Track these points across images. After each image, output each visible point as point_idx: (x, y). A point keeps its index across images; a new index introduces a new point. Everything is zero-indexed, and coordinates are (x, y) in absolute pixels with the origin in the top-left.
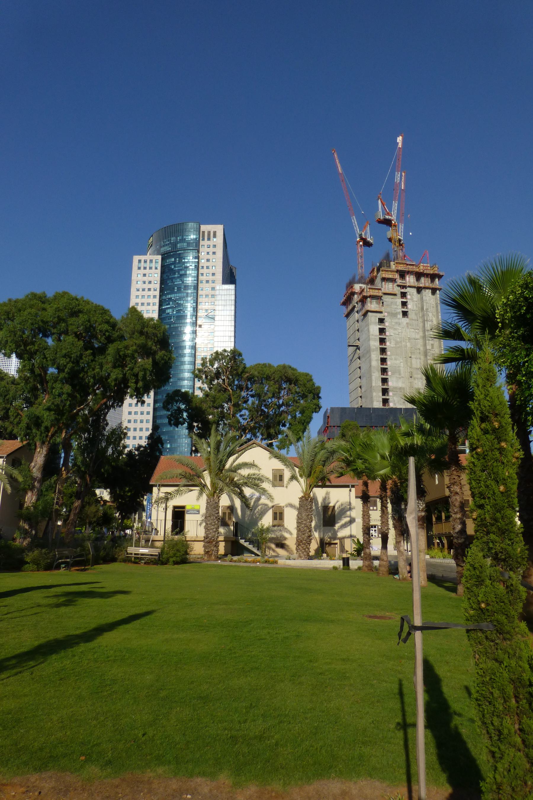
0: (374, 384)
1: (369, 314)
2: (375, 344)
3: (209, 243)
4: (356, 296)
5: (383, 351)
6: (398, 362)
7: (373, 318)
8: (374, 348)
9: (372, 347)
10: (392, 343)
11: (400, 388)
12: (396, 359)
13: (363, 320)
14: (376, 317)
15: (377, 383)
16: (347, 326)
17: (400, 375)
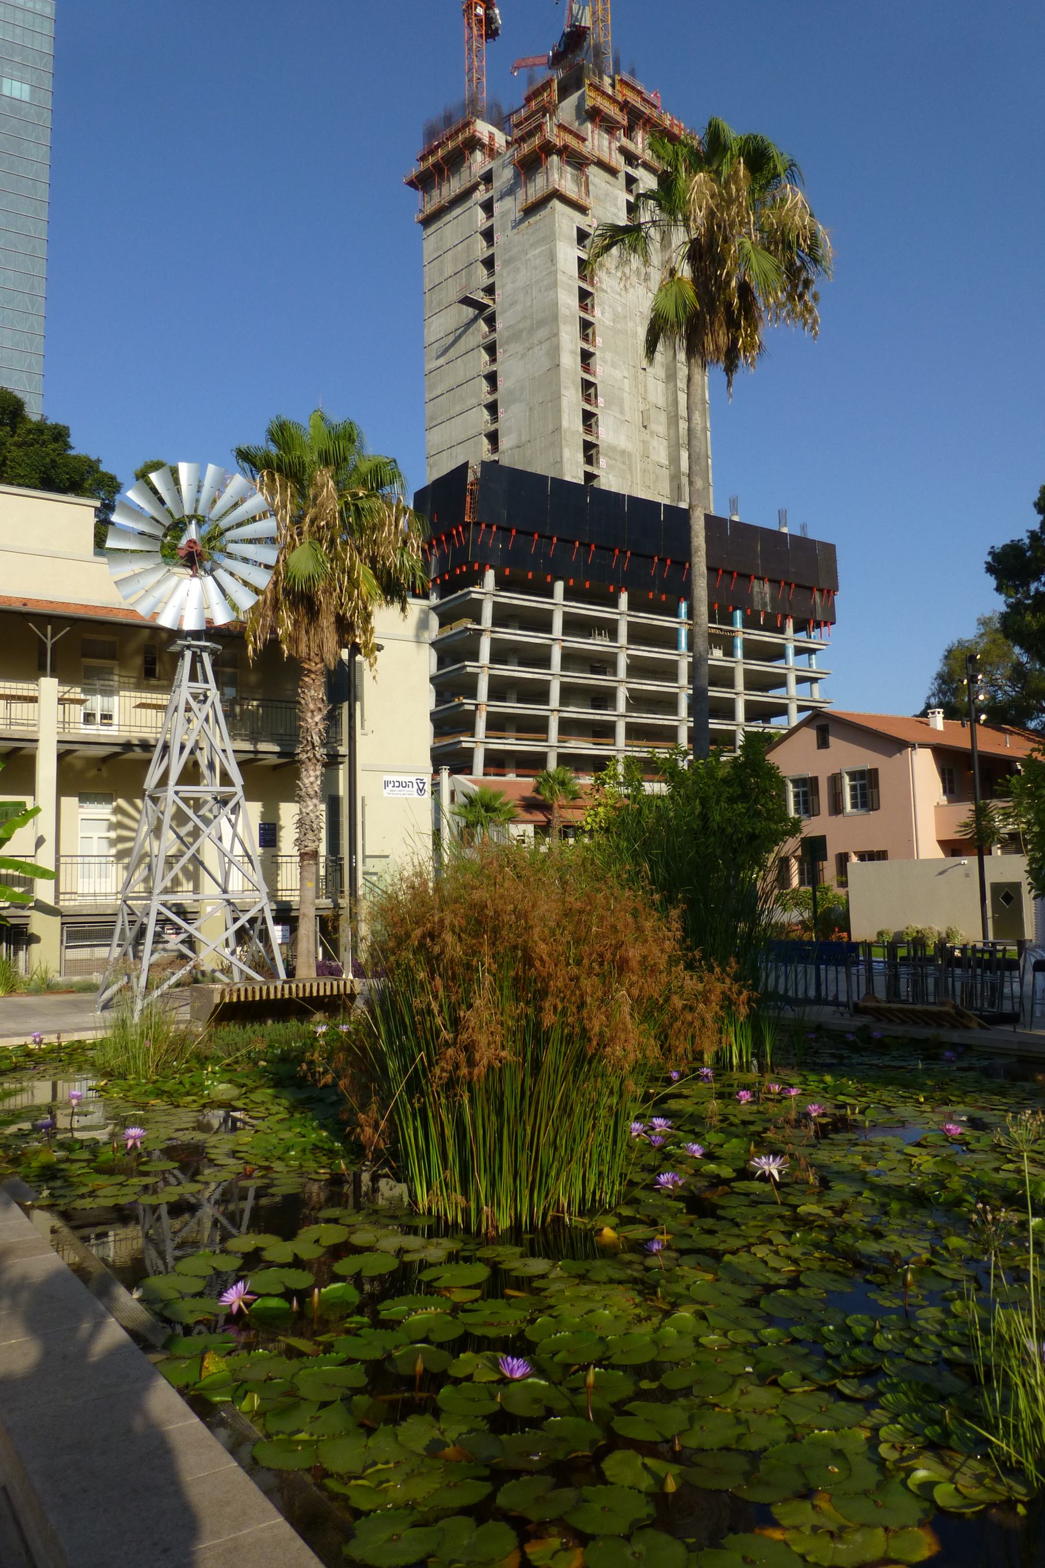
0: (565, 424)
1: (556, 203)
2: (568, 301)
4: (478, 155)
5: (586, 325)
6: (618, 374)
7: (564, 220)
8: (567, 312)
9: (563, 311)
10: (607, 315)
11: (623, 452)
12: (614, 365)
14: (572, 219)
15: (572, 422)
17: (622, 412)
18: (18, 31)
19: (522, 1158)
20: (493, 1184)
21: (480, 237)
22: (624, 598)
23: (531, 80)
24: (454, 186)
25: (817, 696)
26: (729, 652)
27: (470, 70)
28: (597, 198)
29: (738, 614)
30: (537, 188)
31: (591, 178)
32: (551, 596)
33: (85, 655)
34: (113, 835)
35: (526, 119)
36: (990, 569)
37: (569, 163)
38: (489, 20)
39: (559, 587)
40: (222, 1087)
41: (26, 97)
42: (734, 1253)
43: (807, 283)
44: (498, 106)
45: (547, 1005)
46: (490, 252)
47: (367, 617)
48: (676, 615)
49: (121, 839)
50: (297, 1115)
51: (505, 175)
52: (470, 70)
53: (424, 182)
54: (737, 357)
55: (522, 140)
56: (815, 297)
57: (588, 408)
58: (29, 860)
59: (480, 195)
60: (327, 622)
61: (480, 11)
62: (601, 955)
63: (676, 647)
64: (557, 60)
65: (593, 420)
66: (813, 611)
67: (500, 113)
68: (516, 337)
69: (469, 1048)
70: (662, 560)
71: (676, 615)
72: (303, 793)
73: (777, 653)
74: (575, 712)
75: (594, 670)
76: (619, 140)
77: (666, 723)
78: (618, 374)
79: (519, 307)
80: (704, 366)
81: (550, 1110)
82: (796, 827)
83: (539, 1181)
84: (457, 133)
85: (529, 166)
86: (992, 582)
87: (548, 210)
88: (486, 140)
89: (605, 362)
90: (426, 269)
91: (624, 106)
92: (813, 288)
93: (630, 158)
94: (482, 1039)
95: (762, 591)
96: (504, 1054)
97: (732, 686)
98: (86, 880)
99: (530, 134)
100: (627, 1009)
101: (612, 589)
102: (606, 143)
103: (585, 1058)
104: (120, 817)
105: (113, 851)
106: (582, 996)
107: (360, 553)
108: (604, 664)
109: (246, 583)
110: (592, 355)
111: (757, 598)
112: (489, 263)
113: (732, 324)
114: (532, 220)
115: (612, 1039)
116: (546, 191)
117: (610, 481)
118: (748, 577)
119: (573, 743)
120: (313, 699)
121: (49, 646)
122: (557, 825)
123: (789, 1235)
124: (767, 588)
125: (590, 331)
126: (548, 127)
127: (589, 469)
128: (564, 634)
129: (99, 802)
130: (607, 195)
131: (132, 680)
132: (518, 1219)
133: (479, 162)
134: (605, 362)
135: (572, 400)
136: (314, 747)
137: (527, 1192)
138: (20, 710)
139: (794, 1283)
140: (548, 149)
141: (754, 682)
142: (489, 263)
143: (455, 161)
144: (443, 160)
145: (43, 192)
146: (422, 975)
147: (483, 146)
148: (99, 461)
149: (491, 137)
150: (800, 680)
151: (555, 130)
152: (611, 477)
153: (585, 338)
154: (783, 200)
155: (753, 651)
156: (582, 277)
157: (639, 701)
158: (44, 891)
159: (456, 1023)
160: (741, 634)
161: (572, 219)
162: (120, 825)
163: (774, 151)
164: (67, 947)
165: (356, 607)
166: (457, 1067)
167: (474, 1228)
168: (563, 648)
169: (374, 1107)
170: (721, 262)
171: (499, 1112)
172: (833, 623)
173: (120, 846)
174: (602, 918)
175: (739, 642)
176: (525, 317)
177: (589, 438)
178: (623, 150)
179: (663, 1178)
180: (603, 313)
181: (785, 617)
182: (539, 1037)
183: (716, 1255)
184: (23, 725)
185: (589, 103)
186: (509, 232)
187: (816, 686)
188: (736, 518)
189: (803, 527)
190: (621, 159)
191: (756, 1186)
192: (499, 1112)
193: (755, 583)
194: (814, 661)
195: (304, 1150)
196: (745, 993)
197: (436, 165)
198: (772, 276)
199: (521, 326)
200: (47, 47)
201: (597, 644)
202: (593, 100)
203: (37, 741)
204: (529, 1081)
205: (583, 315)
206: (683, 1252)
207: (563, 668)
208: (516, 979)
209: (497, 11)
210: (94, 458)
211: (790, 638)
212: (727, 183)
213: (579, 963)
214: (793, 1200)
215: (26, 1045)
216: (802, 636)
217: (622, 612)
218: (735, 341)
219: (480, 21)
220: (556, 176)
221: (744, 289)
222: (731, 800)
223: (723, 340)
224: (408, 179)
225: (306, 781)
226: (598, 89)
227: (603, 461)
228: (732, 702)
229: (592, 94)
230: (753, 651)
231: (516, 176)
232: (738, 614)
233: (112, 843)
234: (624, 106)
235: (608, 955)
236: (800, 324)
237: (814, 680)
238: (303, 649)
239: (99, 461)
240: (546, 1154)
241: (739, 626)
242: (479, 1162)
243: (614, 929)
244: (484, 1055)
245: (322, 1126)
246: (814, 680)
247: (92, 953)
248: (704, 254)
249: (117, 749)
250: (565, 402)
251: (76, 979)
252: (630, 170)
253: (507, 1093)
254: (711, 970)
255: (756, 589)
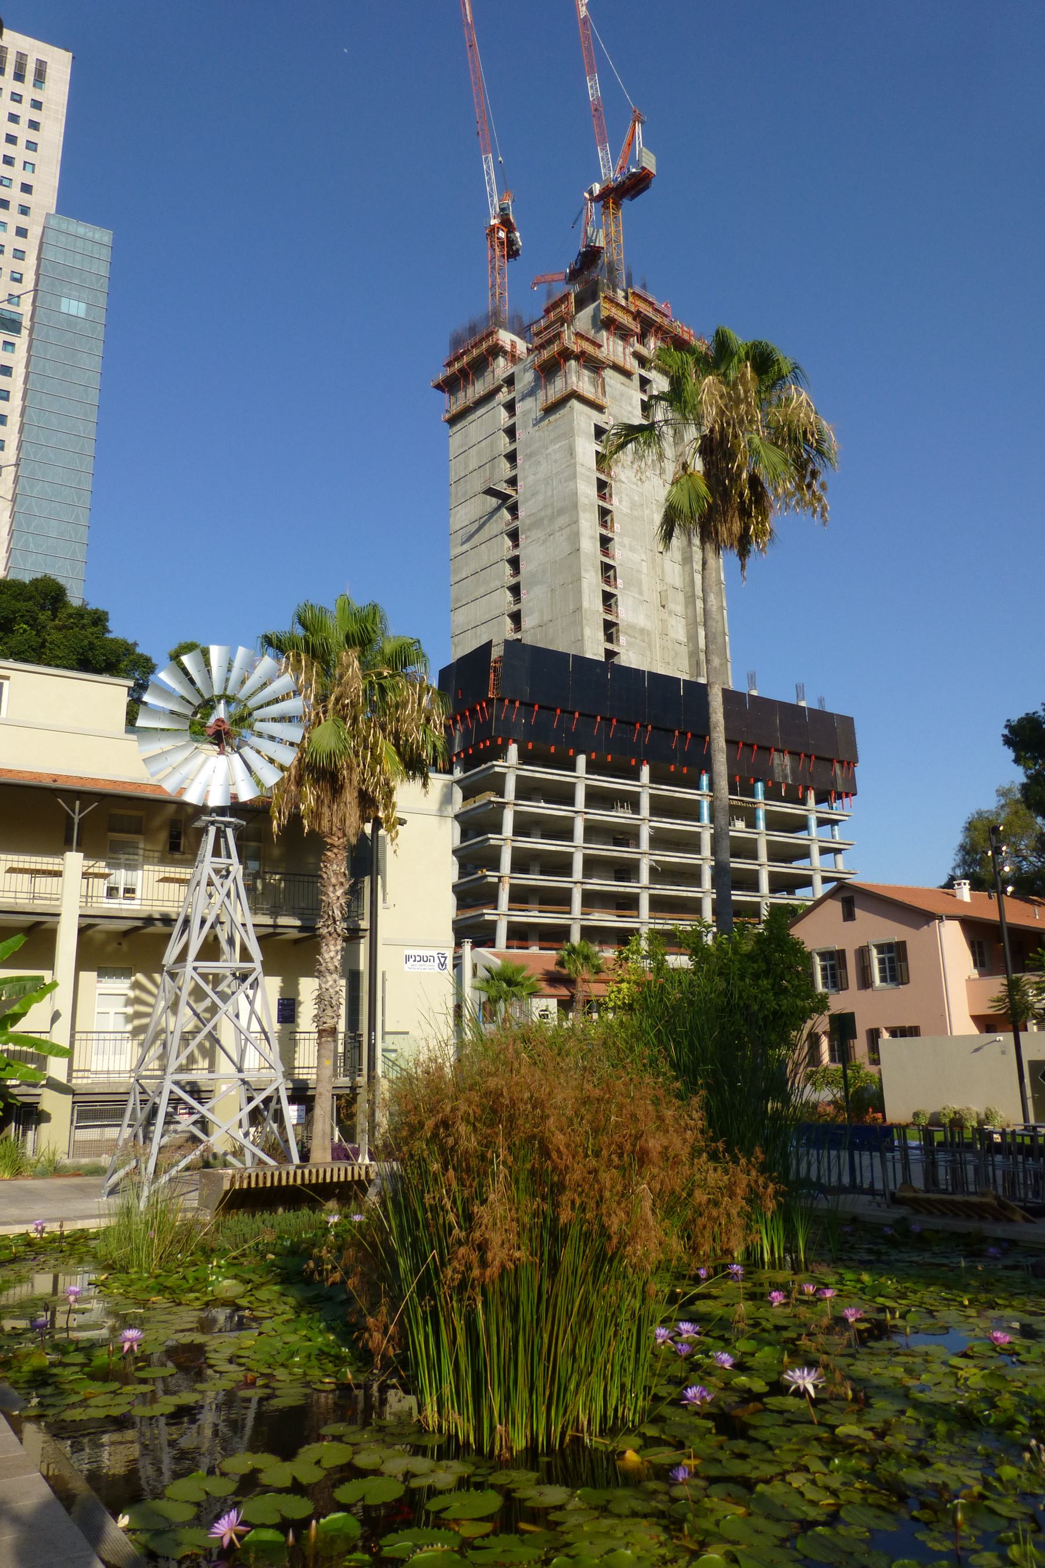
0: (586, 604)
1: (575, 403)
2: (587, 491)
3: (18, 87)
4: (501, 361)
5: (604, 513)
6: (636, 558)
7: (583, 418)
8: (586, 501)
9: (582, 500)
11: (642, 631)
12: (632, 549)
13: (538, 422)
14: (589, 417)
16: (452, 449)
17: (641, 593)
18: (78, 257)
19: (539, 1371)
20: (507, 1399)
21: (503, 434)
22: (645, 771)
23: (549, 295)
24: (478, 388)
25: (841, 867)
26: (752, 824)
27: (493, 286)
28: (613, 398)
29: (760, 786)
30: (557, 389)
31: (607, 380)
32: (574, 770)
33: (112, 829)
34: (130, 1010)
35: (546, 328)
36: (1008, 741)
37: (586, 367)
38: (511, 242)
39: (581, 760)
40: (227, 1283)
41: (82, 314)
42: (767, 1482)
43: (814, 474)
44: (520, 318)
45: (564, 1199)
46: (512, 447)
47: (389, 793)
48: (697, 786)
49: (138, 1015)
50: (304, 1316)
51: (526, 379)
52: (493, 286)
53: (450, 385)
54: (749, 543)
55: (542, 347)
56: (823, 486)
57: (608, 589)
58: (43, 1036)
59: (503, 396)
60: (350, 796)
61: (502, 234)
62: (620, 1146)
63: (698, 819)
64: (574, 276)
65: (613, 601)
66: (834, 783)
67: (521, 324)
68: (537, 524)
69: (482, 1248)
70: (683, 734)
71: (697, 786)
72: (323, 969)
73: (800, 824)
74: (599, 884)
75: (617, 843)
76: (633, 346)
77: (690, 894)
78: (636, 558)
79: (540, 497)
80: (718, 549)
81: (569, 1316)
82: (822, 1004)
83: (557, 1396)
84: (480, 342)
85: (548, 370)
86: (1010, 754)
87: (567, 409)
88: (508, 348)
89: (624, 546)
90: (452, 463)
91: (637, 316)
92: (821, 478)
93: (643, 361)
94: (496, 1238)
95: (782, 764)
96: (517, 1254)
97: (756, 858)
98: (100, 1057)
99: (550, 342)
100: (648, 1204)
101: (633, 762)
102: (621, 349)
103: (604, 1258)
104: (137, 992)
105: (129, 1027)
106: (601, 1190)
107: (383, 729)
108: (626, 836)
109: (271, 761)
110: (610, 540)
111: (777, 770)
112: (512, 457)
113: (744, 513)
114: (552, 418)
115: (633, 1237)
116: (565, 392)
117: (630, 657)
118: (769, 749)
119: (596, 916)
120: (336, 874)
121: (76, 821)
122: (580, 997)
123: (827, 1460)
124: (787, 760)
125: (608, 518)
126: (565, 336)
127: (609, 646)
128: (586, 807)
129: (118, 976)
130: (622, 395)
131: (157, 854)
132: (534, 1439)
133: (501, 367)
134: (624, 546)
135: (592, 583)
136: (335, 922)
137: (544, 1409)
138: (43, 884)
139: (833, 1519)
140: (566, 355)
141: (778, 853)
142: (512, 457)
143: (480, 366)
144: (467, 367)
145: (94, 397)
146: (436, 1167)
147: (505, 353)
148: (136, 644)
149: (513, 345)
150: (824, 851)
151: (573, 337)
152: (631, 654)
153: (604, 524)
154: (789, 400)
155: (775, 822)
156: (600, 469)
157: (659, 873)
158: (57, 1068)
159: (468, 1219)
160: (762, 804)
161: (589, 417)
162: (137, 1001)
163: (779, 355)
164: (77, 1128)
165: (378, 783)
166: (469, 1267)
167: (486, 1449)
168: (586, 820)
169: (384, 1309)
170: (731, 456)
171: (514, 1318)
172: (855, 794)
173: (137, 1022)
174: (621, 1107)
175: (761, 814)
176: (545, 507)
177: (609, 618)
178: (636, 355)
179: (691, 1393)
180: (620, 501)
181: (806, 788)
182: (557, 1235)
183: (748, 1484)
184: (46, 899)
185: (604, 314)
186: (530, 429)
187: (839, 857)
188: (754, 693)
189: (821, 701)
190: (635, 363)
191: (790, 1402)
192: (514, 1318)
193: (775, 754)
194: (836, 832)
195: (309, 1356)
196: (771, 1186)
197: (461, 370)
198: (781, 468)
199: (542, 514)
200: (104, 270)
201: (619, 816)
202: (608, 311)
203: (59, 915)
204: (546, 1285)
205: (601, 503)
206: (713, 1480)
207: (586, 841)
208: (532, 1172)
209: (518, 234)
210: (130, 641)
211: (812, 809)
212: (735, 384)
213: (597, 1154)
214: (830, 1420)
215: (27, 1233)
216: (824, 807)
217: (643, 785)
218: (746, 529)
219: (502, 243)
220: (574, 379)
221: (754, 481)
222: (756, 977)
223: (737, 527)
224: (436, 382)
225: (326, 956)
226: (612, 301)
227: (623, 639)
228: (756, 873)
229: (607, 306)
230: (775, 822)
231: (537, 379)
232: (760, 786)
233: (129, 1019)
234: (637, 316)
235: (628, 1147)
236: (809, 512)
237: (838, 851)
238: (325, 824)
239: (136, 644)
240: (564, 1364)
241: (760, 797)
242: (493, 1374)
243: (634, 1117)
244: (497, 1255)
245: (330, 1329)
246: (838, 851)
247: (102, 1133)
248: (715, 449)
249: (139, 923)
250: (585, 584)
251: (84, 1161)
252: (643, 372)
253: (523, 1298)
254: (736, 1161)
255: (776, 761)
